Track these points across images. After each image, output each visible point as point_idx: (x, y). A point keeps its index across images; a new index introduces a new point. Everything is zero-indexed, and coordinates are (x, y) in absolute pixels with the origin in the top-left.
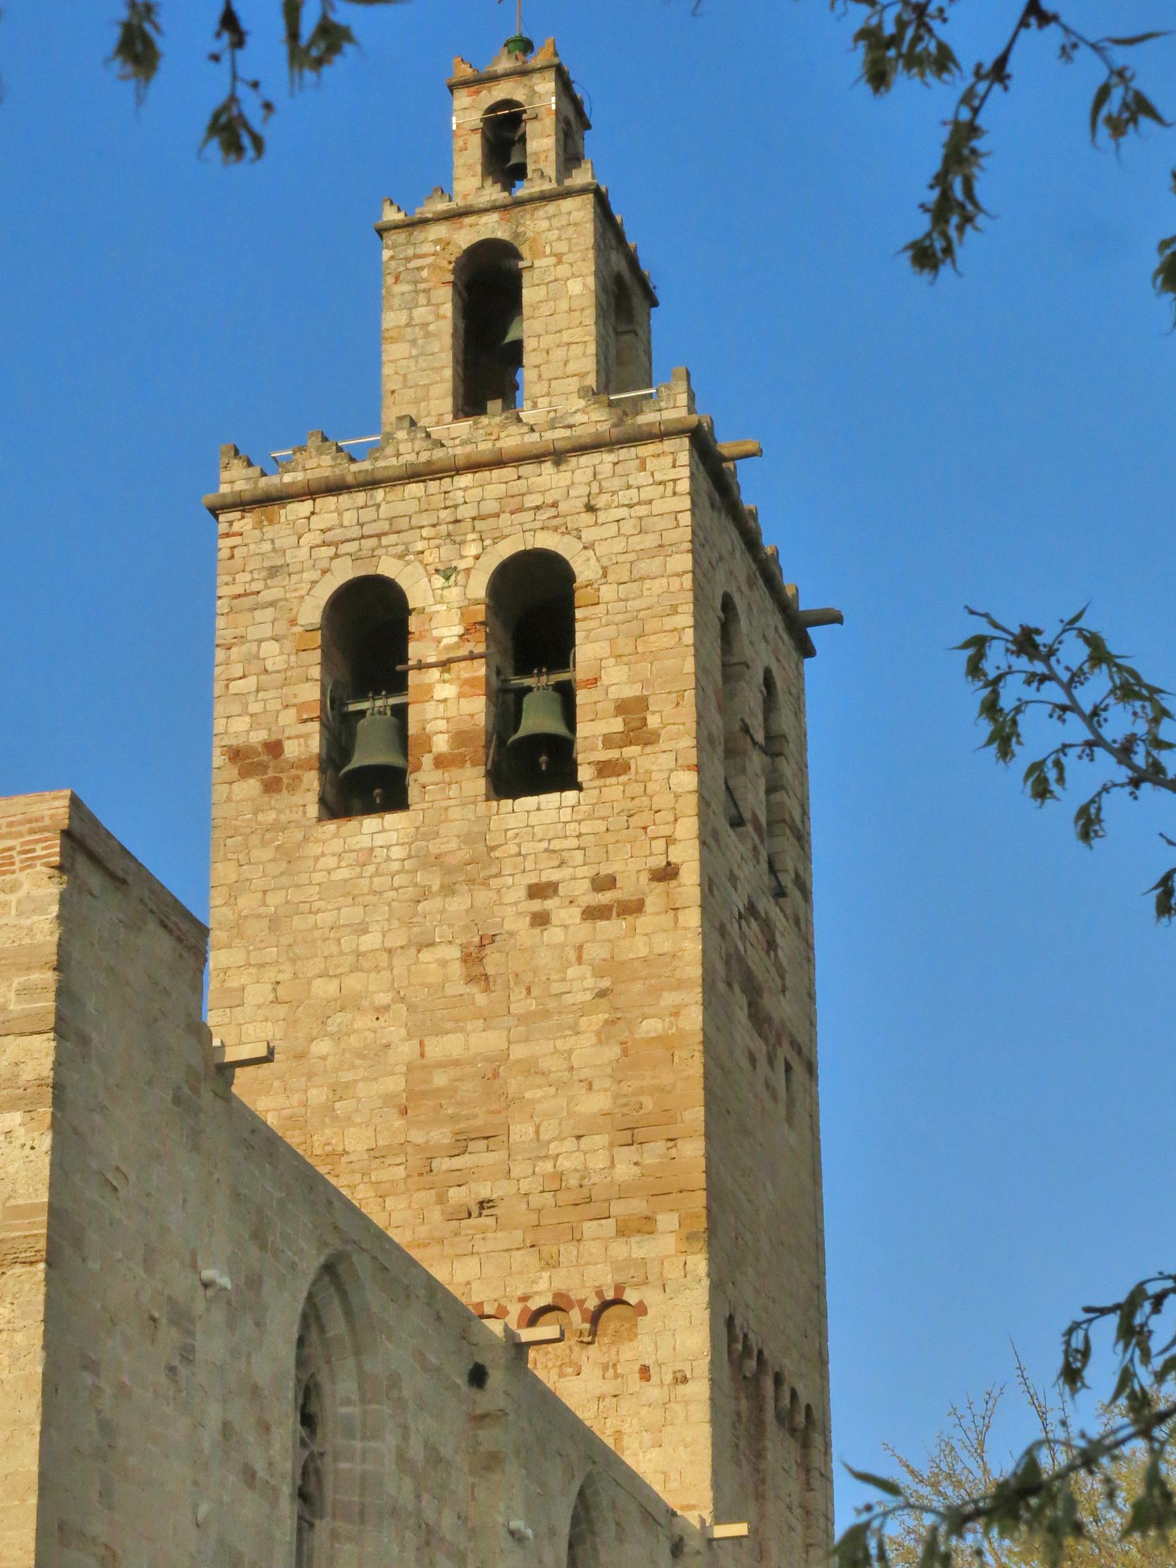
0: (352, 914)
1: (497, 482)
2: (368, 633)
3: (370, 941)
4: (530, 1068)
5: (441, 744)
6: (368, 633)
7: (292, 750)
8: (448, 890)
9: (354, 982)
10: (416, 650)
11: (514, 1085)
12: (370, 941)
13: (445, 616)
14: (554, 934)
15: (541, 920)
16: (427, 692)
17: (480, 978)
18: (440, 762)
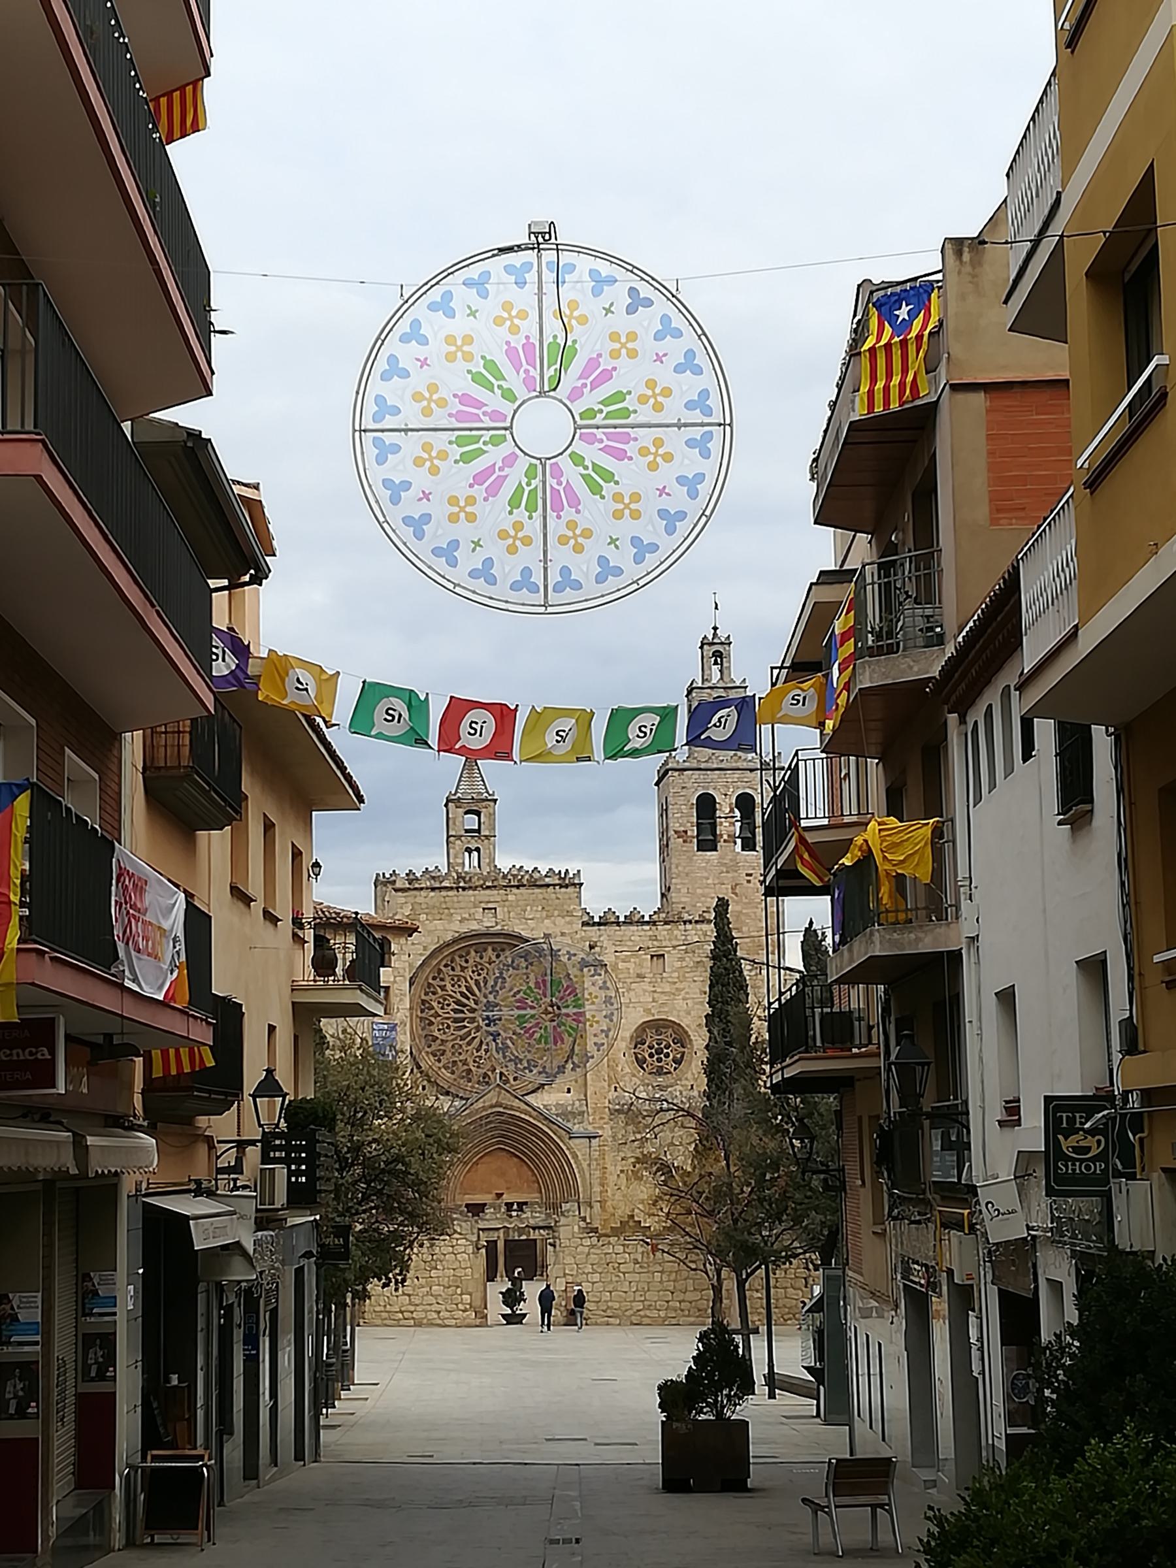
0: (706, 874)
1: (737, 774)
2: (706, 806)
3: (709, 881)
4: (747, 914)
5: (725, 837)
6: (706, 806)
7: (689, 833)
8: (727, 872)
9: (707, 890)
10: (718, 813)
11: (743, 918)
12: (709, 881)
13: (725, 806)
14: (751, 885)
15: (749, 881)
16: (721, 823)
17: (736, 894)
18: (725, 841)
